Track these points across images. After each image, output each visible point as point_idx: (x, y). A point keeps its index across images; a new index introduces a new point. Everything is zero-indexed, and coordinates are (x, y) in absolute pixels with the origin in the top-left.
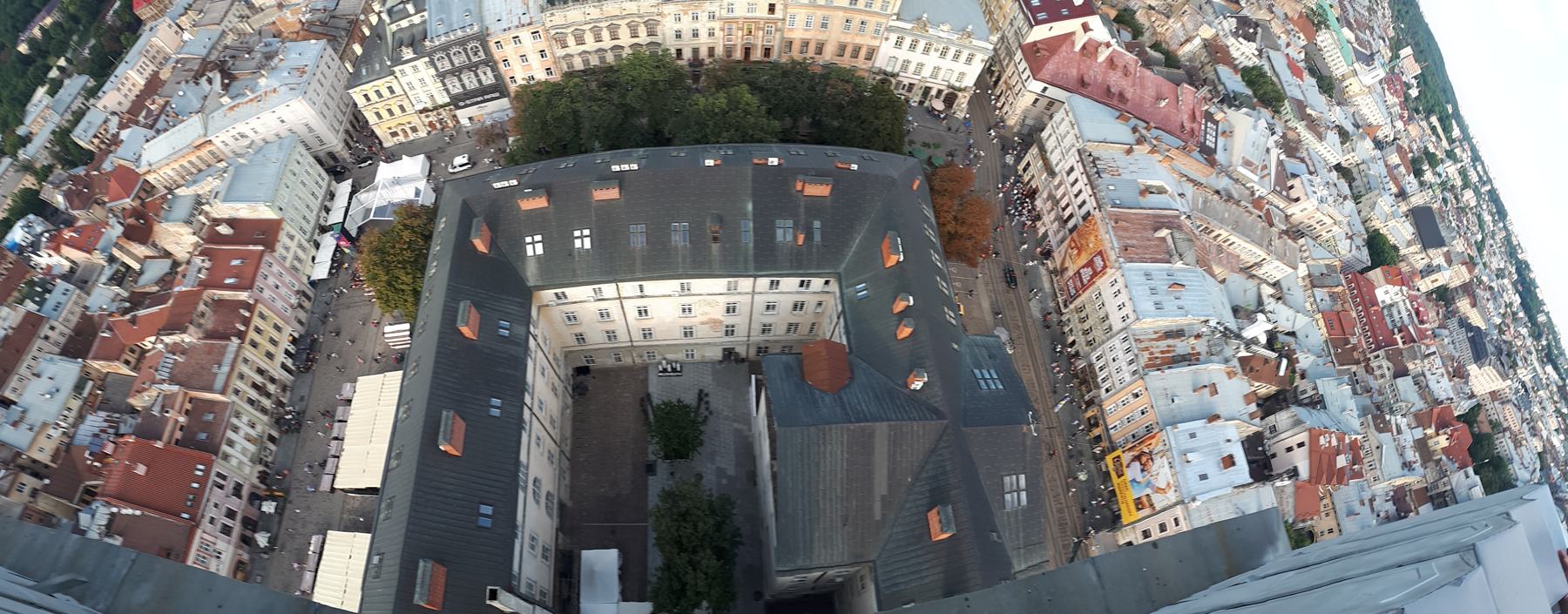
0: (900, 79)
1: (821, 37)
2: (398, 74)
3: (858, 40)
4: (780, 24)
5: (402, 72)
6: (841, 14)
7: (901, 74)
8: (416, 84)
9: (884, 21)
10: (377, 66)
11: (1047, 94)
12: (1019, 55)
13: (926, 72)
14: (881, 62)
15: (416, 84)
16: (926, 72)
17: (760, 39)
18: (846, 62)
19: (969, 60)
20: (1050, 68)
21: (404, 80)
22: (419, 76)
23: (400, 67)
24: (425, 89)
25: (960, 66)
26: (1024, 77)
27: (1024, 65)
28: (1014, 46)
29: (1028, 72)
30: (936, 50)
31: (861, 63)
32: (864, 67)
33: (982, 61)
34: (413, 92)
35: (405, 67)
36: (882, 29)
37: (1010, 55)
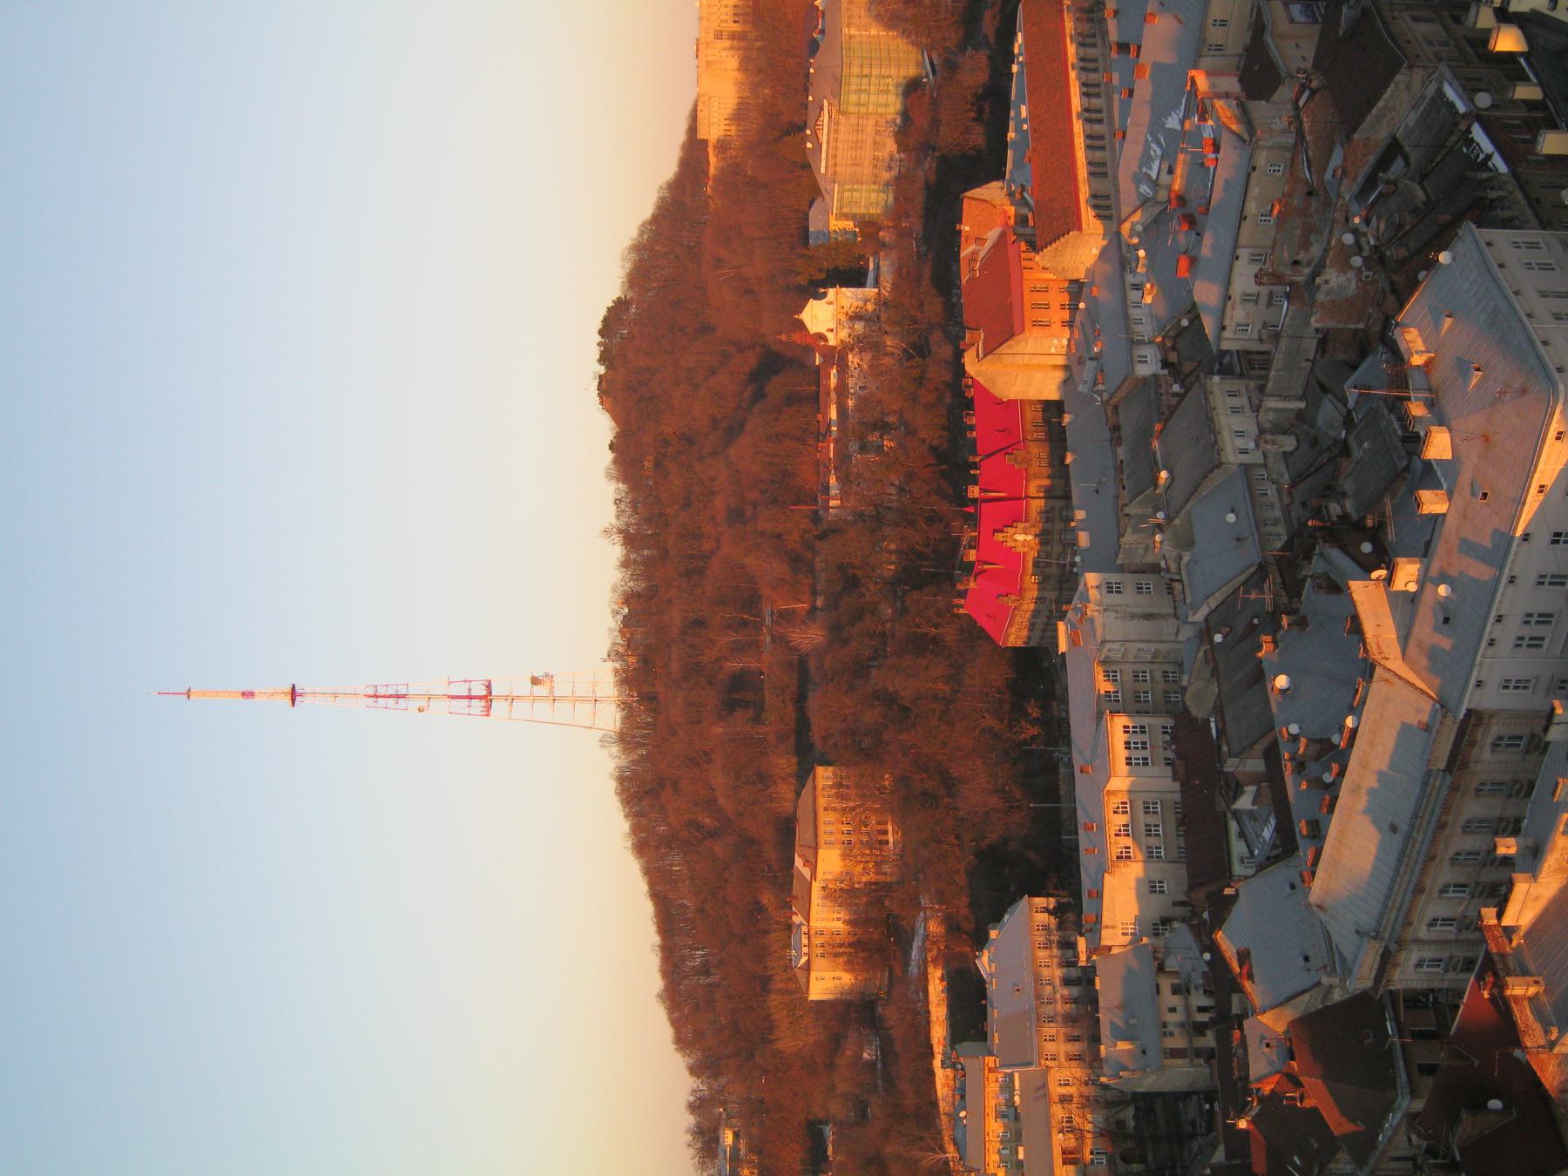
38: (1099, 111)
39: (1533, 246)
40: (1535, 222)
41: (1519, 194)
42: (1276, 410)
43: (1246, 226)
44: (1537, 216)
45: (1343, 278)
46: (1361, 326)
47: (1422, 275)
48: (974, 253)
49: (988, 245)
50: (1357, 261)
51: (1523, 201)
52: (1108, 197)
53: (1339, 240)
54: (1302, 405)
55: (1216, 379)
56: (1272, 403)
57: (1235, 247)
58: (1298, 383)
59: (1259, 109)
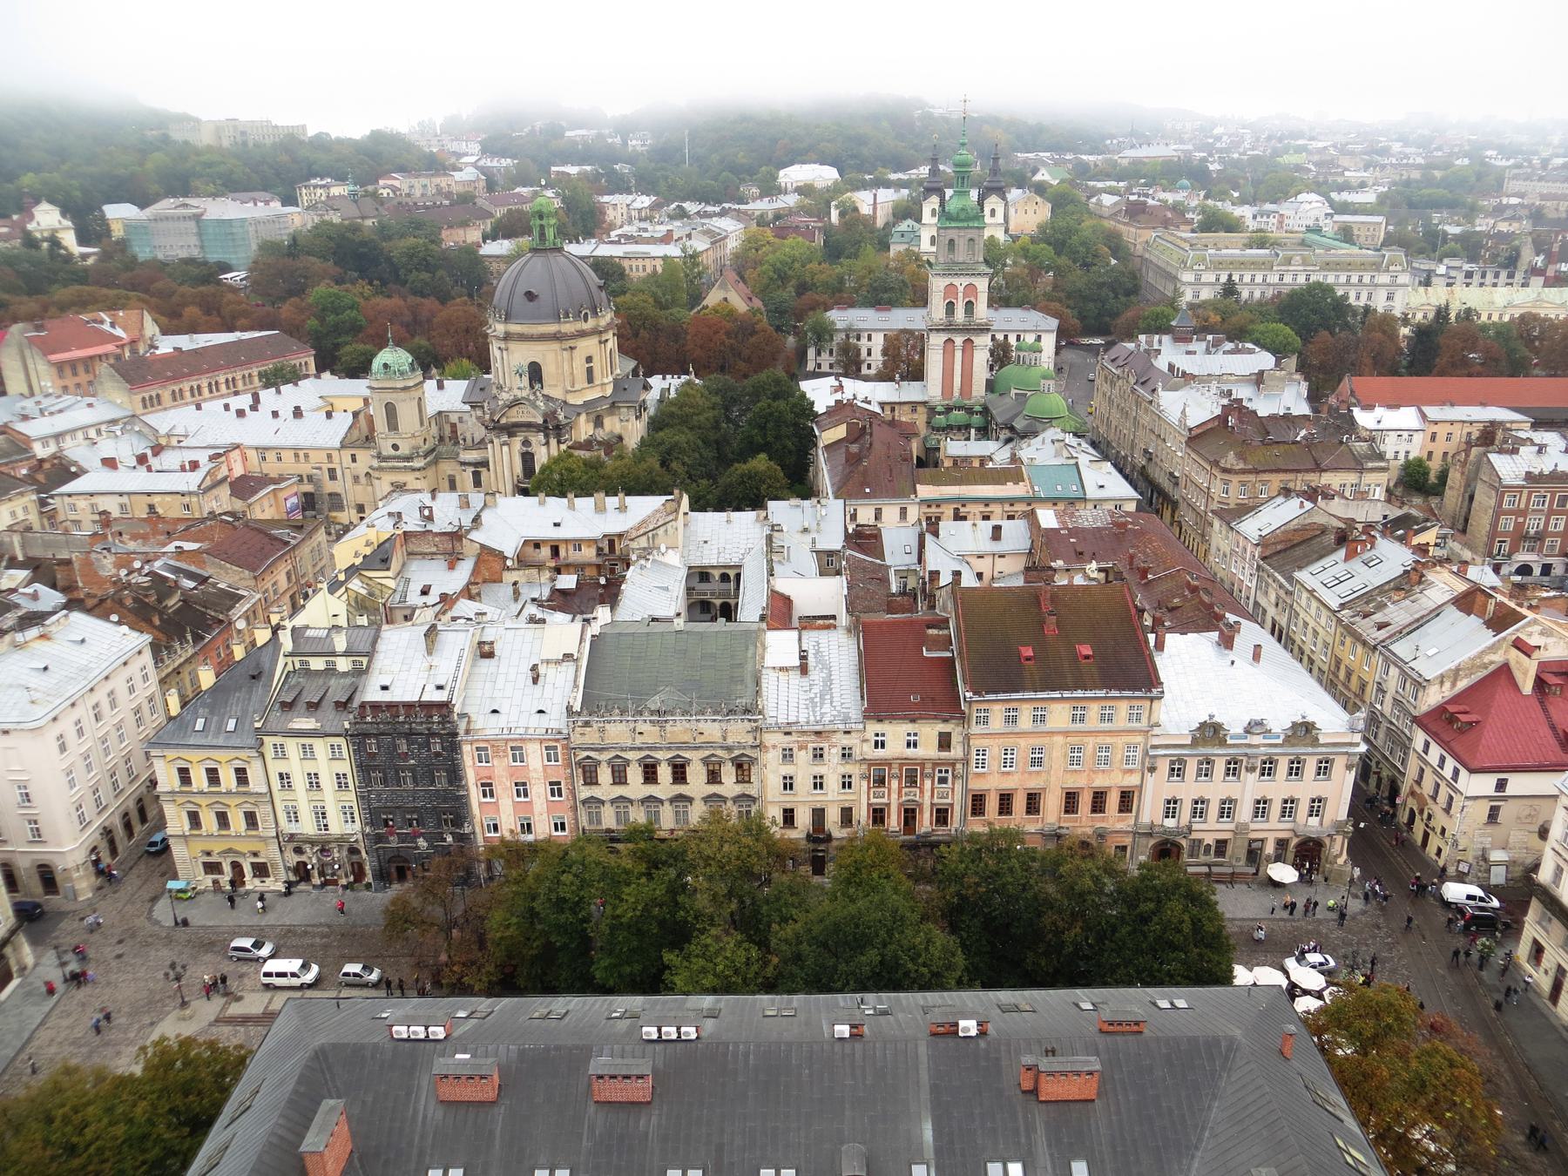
0: (1194, 836)
1: (1034, 784)
2: (269, 752)
3: (1100, 782)
4: (959, 766)
5: (280, 752)
6: (1059, 739)
7: (1195, 827)
8: (299, 782)
9: (1139, 739)
10: (231, 725)
11: (1510, 791)
12: (1419, 738)
13: (1244, 813)
14: (1150, 811)
15: (299, 782)
16: (1244, 813)
17: (927, 794)
18: (1084, 823)
19: (1324, 769)
20: (1491, 740)
21: (275, 767)
22: (310, 767)
23: (278, 740)
24: (315, 795)
25: (1306, 788)
26: (1448, 772)
27: (1435, 752)
28: (1403, 724)
29: (1450, 763)
30: (1251, 769)
31: (1112, 819)
32: (1119, 826)
33: (1349, 767)
34: (287, 795)
35: (292, 745)
36: (1139, 754)
37: (1404, 745)
38: (218, 390)
39: (145, 678)
40: (163, 675)
41: (182, 660)
42: (12, 542)
43: (145, 497)
44: (168, 675)
45: (110, 566)
46: (80, 584)
47: (114, 618)
48: (102, 322)
49: (112, 330)
50: (123, 572)
51: (176, 664)
52: (159, 404)
53: (135, 559)
54: (20, 558)
55: (34, 497)
56: (16, 539)
57: (129, 494)
58: (37, 552)
59: (224, 491)
